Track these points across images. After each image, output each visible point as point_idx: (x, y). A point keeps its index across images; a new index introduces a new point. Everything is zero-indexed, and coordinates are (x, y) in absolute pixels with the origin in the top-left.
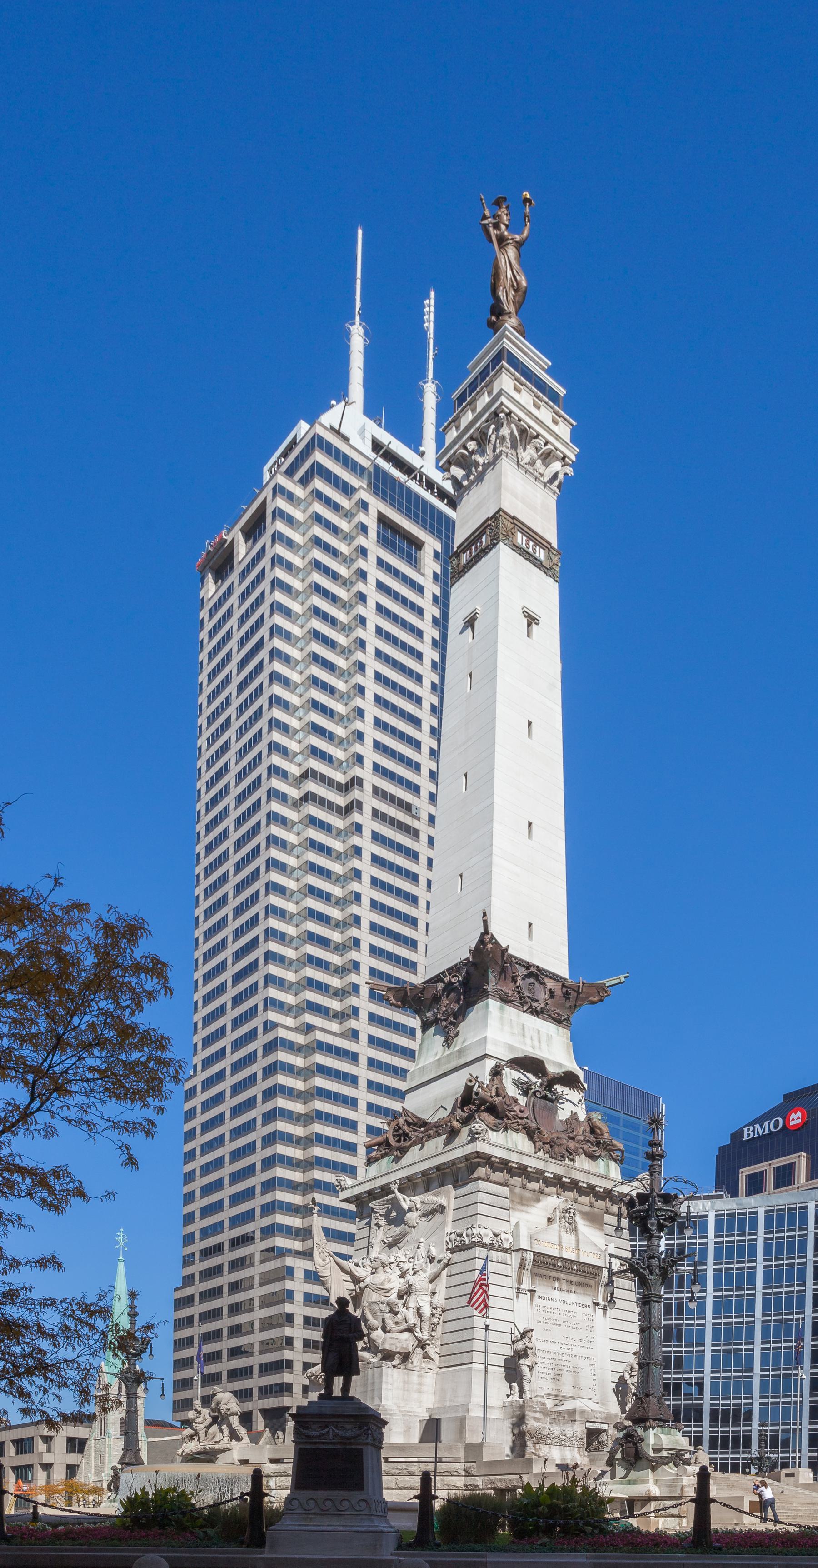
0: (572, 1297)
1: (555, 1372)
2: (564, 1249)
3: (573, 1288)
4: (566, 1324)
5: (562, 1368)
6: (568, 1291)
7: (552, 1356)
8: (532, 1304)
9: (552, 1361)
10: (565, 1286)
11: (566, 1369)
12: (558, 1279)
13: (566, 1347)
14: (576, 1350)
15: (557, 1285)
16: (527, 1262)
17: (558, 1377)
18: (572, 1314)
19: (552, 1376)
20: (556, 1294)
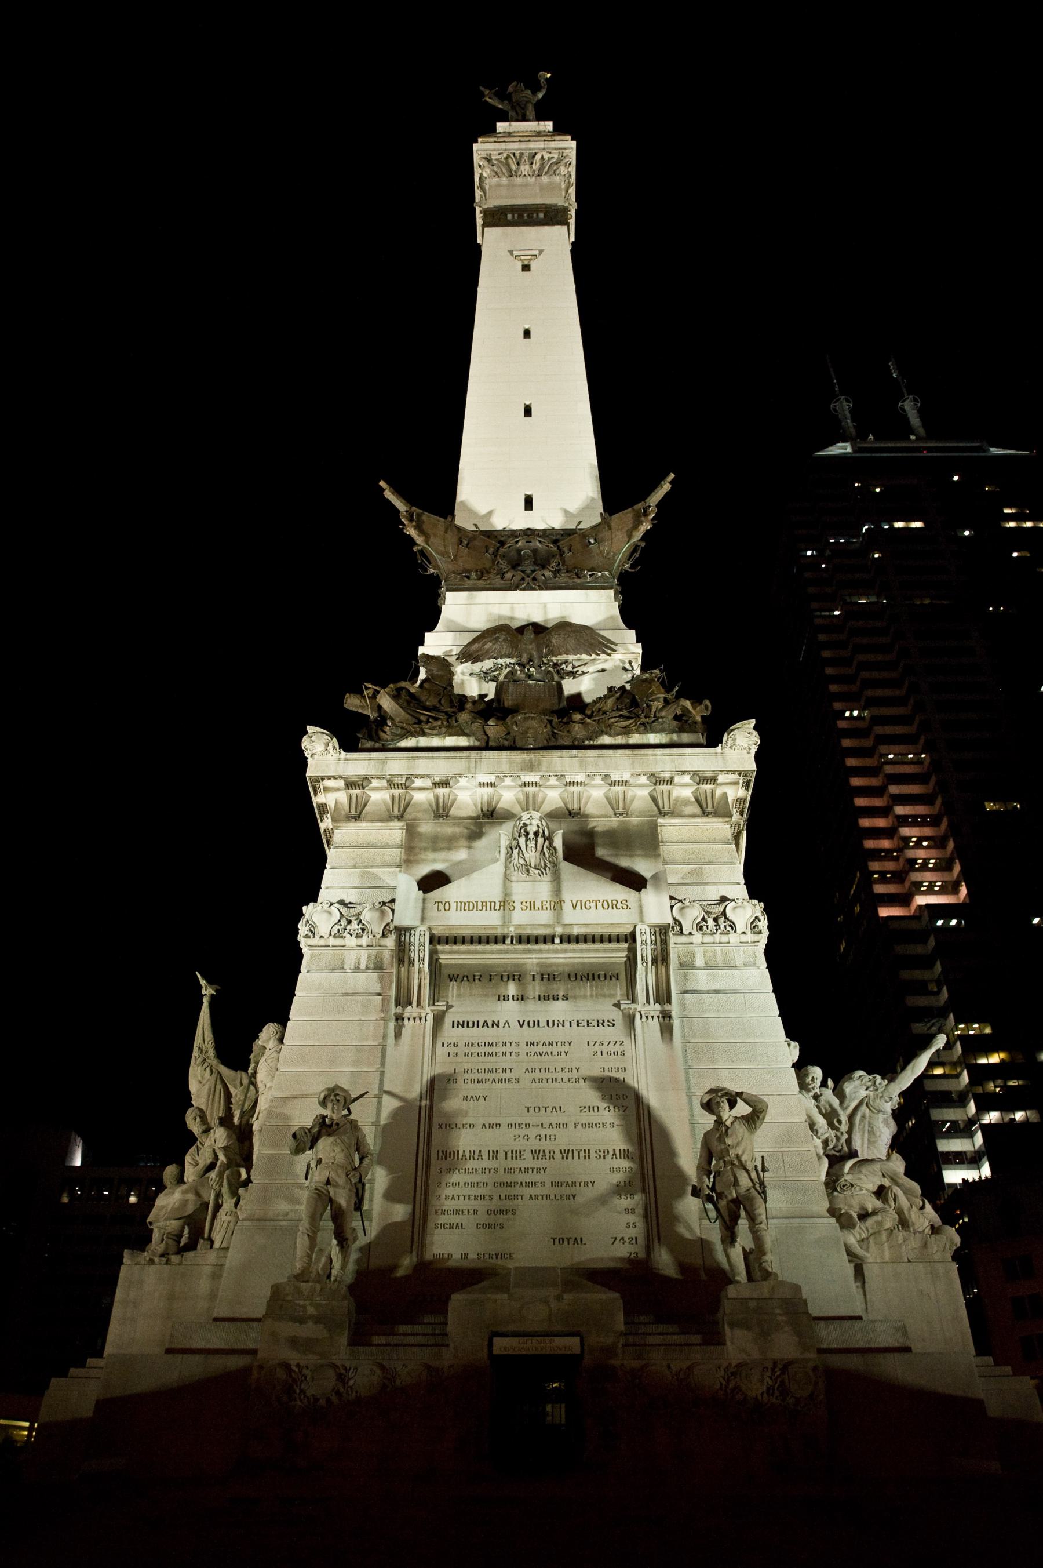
0: (559, 1009)
1: (495, 1205)
4: (537, 1075)
5: (518, 1190)
7: (486, 1163)
8: (434, 1043)
9: (484, 1178)
10: (536, 988)
11: (532, 1191)
13: (533, 1132)
14: (564, 1139)
15: (512, 989)
16: (415, 955)
17: (500, 1219)
18: (554, 1049)
19: (482, 1218)
20: (510, 1011)
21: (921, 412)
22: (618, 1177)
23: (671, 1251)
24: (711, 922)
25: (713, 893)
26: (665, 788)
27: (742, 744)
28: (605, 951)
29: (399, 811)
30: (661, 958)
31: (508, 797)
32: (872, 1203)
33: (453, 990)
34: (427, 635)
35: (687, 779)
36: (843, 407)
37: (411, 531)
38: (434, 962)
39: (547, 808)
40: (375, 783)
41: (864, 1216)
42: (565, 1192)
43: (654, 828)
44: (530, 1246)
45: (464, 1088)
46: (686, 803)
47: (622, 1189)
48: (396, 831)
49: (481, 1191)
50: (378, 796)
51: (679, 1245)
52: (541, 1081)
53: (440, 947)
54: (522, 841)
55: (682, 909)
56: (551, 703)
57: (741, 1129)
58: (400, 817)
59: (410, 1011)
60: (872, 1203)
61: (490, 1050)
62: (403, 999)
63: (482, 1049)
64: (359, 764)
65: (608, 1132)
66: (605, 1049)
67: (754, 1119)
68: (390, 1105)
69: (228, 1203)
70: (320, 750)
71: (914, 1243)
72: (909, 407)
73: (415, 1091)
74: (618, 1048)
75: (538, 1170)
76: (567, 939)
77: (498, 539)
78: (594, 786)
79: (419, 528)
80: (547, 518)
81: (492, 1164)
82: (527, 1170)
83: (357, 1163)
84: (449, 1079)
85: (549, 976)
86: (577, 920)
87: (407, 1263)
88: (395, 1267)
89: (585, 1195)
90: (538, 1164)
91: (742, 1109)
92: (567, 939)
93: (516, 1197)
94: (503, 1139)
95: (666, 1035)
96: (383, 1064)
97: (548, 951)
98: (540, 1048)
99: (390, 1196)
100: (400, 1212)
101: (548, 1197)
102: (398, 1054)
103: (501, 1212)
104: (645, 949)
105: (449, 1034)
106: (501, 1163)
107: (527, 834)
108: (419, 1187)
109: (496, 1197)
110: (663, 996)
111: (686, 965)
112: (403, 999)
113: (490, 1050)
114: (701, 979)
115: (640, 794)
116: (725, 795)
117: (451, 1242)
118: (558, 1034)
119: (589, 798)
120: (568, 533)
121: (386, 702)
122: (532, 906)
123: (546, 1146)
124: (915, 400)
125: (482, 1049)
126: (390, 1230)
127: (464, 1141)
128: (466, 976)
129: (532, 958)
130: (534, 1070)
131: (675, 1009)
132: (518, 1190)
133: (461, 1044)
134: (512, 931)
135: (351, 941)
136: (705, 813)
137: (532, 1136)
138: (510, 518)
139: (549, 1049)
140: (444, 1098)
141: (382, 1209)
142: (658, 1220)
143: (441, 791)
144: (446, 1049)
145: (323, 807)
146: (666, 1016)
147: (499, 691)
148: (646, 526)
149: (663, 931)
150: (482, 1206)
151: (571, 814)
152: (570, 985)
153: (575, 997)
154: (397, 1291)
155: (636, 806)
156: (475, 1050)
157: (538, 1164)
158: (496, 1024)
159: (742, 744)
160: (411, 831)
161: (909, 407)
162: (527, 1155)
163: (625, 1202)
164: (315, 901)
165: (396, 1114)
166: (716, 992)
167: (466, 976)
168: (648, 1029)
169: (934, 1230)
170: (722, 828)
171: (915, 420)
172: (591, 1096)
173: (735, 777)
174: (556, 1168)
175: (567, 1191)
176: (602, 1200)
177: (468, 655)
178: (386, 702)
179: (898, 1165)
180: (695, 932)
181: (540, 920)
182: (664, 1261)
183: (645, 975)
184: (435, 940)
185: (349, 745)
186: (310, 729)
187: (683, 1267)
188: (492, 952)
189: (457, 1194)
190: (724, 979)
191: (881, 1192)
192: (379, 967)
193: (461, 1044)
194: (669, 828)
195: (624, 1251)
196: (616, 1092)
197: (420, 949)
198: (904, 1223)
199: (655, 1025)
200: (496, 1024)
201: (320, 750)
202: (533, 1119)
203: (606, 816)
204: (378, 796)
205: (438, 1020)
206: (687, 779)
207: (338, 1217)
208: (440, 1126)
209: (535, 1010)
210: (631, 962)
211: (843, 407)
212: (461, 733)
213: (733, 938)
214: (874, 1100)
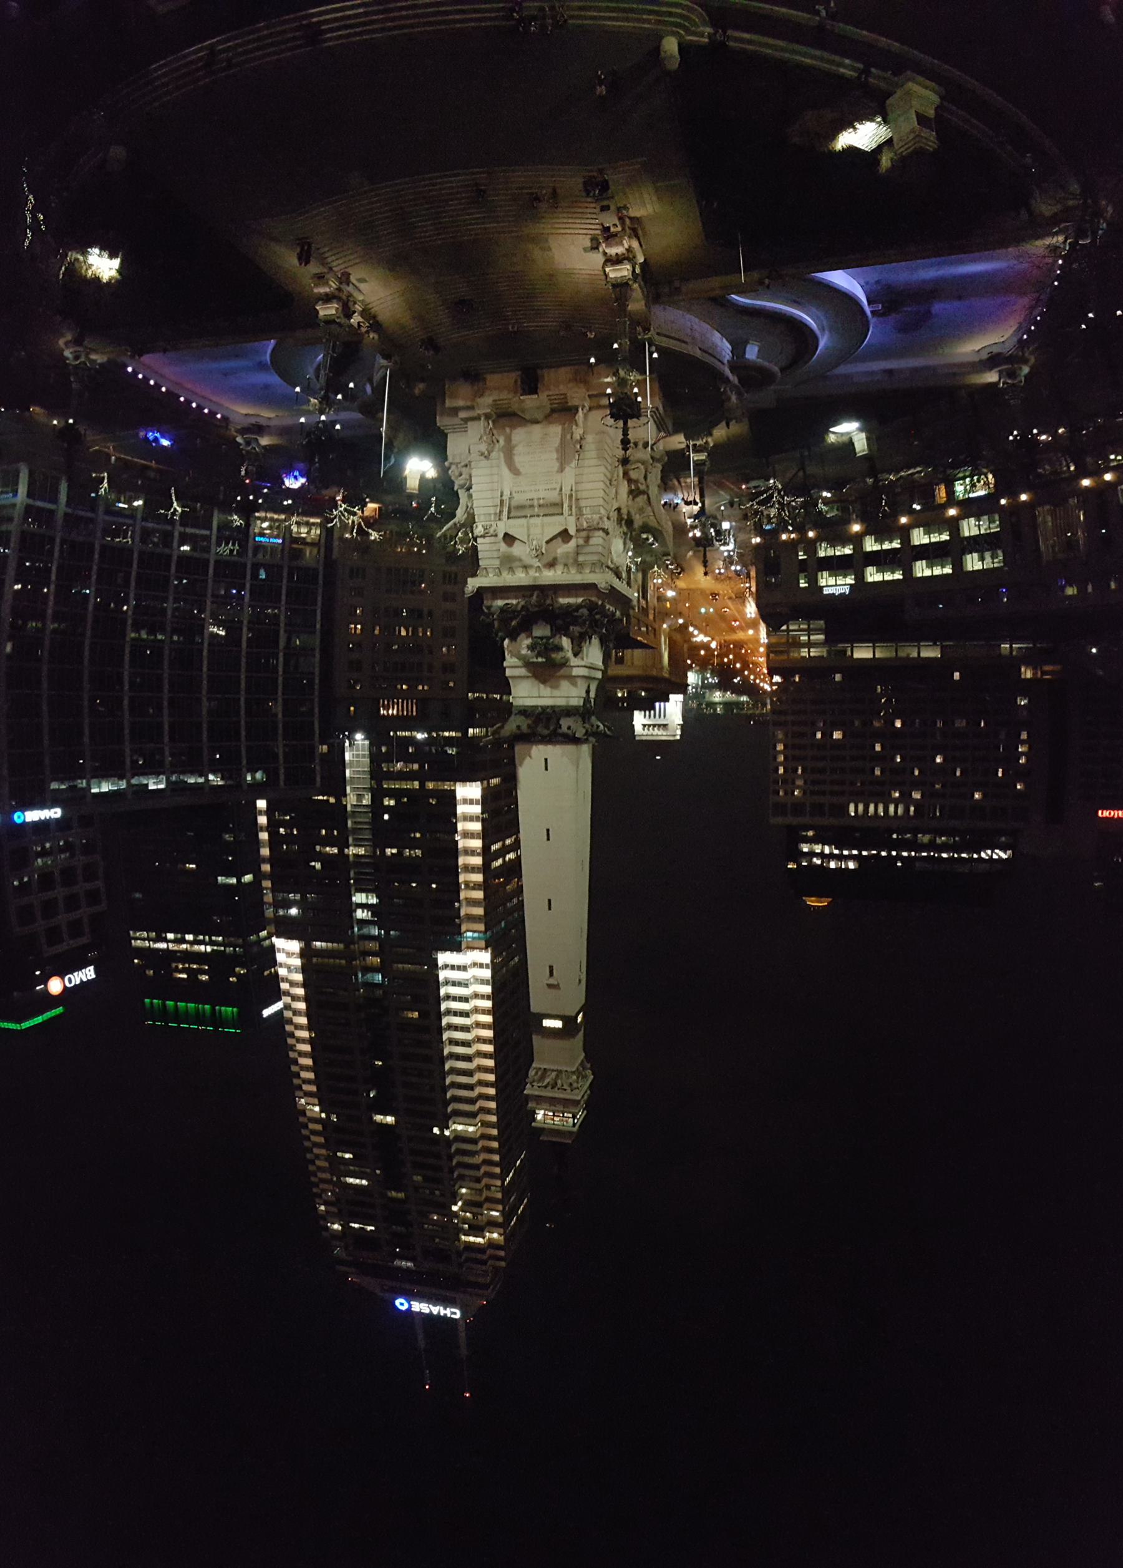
3: (529, 502)
10: (536, 503)
15: (541, 502)
20: (542, 494)
25: (487, 540)
44: (537, 429)
47: (516, 446)
65: (518, 460)
73: (567, 469)
80: (539, 752)
86: (523, 521)
92: (526, 517)
104: (505, 513)
110: (502, 502)
114: (492, 510)
115: (505, 574)
117: (555, 430)
127: (555, 456)
128: (555, 505)
142: (508, 440)
168: (507, 493)
181: (533, 520)
182: (508, 430)
183: (506, 510)
189: (556, 441)
194: (497, 562)
196: (515, 472)
209: (535, 495)
210: (509, 512)
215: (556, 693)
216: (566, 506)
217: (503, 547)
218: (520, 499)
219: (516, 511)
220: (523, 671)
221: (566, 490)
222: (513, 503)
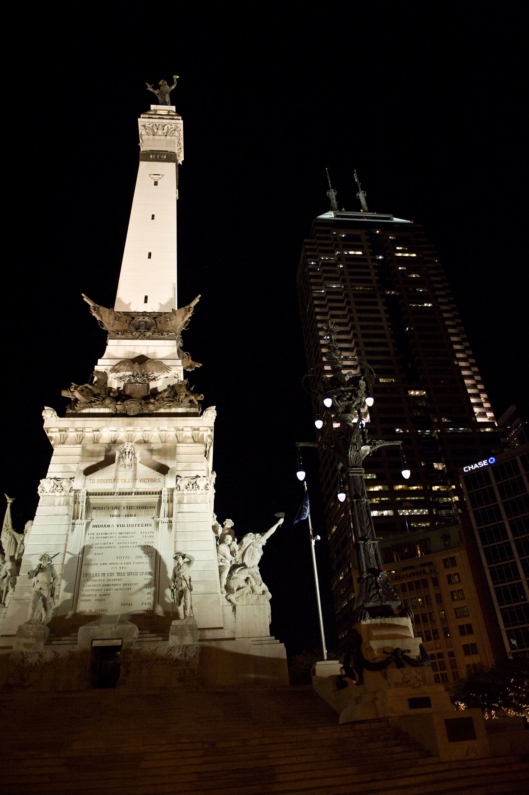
0: (132, 520)
1: (103, 592)
2: (120, 481)
4: (122, 545)
5: (111, 587)
6: (128, 516)
7: (101, 578)
8: (85, 533)
10: (124, 512)
11: (116, 587)
12: (118, 508)
14: (129, 568)
15: (116, 512)
18: (129, 535)
19: (98, 597)
20: (114, 521)
21: (366, 199)
22: (147, 582)
23: (162, 607)
24: (191, 486)
26: (181, 432)
27: (211, 414)
28: (151, 498)
29: (80, 441)
30: (171, 501)
31: (121, 435)
32: (243, 584)
33: (94, 514)
34: (99, 360)
35: (189, 429)
36: (332, 194)
37: (94, 314)
38: (88, 503)
39: (136, 440)
40: (70, 430)
41: (238, 589)
42: (127, 587)
43: (175, 447)
45: (94, 550)
46: (188, 438)
47: (147, 586)
48: (78, 449)
49: (98, 588)
50: (72, 435)
51: (164, 604)
52: (123, 547)
53: (90, 497)
54: (124, 455)
55: (181, 481)
56: (144, 393)
57: (185, 566)
58: (80, 443)
59: (78, 521)
60: (243, 584)
61: (105, 536)
62: (75, 517)
63: (103, 536)
64: (65, 422)
65: (145, 565)
66: (147, 535)
67: (189, 563)
68: (68, 556)
69: (11, 590)
70: (49, 417)
71: (255, 597)
72: (361, 196)
73: (77, 551)
74: (152, 534)
75: (119, 580)
76: (137, 493)
77: (130, 316)
78: (154, 431)
79: (98, 313)
81: (103, 578)
82: (115, 580)
83: (52, 581)
84: (90, 547)
85: (130, 508)
86: (142, 487)
87: (70, 613)
88: (66, 615)
89: (134, 588)
90: (119, 577)
91: (186, 560)
92: (137, 493)
93: (110, 590)
94: (107, 569)
95: (170, 529)
96: (67, 541)
97: (130, 498)
98: (124, 535)
99: (66, 590)
100: (69, 596)
101: (121, 589)
102: (72, 537)
103: (104, 595)
104: (165, 497)
105: (91, 530)
106: (106, 577)
107: (126, 452)
108: (76, 588)
109: (103, 590)
111: (180, 502)
112: (75, 517)
113: (105, 536)
114: (185, 507)
115: (172, 434)
116: (203, 435)
117: (86, 606)
118: (131, 529)
119: (152, 436)
120: (160, 314)
121: (77, 395)
122: (125, 481)
123: (123, 571)
124: (364, 193)
125: (103, 536)
126: (66, 602)
127: (93, 570)
128: (100, 508)
129: (124, 501)
130: (121, 543)
131: (173, 519)
132: (111, 587)
133: (95, 534)
134: (117, 491)
135: (58, 494)
136: (195, 442)
137: (118, 568)
138: (137, 306)
139: (127, 535)
140: (88, 554)
141: (63, 595)
142: (158, 597)
143: (96, 433)
144: (90, 536)
145: (51, 437)
146: (170, 522)
147: (124, 387)
148: (189, 315)
149: (172, 490)
150: (98, 593)
151: (145, 442)
152: (137, 510)
153: (138, 515)
154: (64, 624)
155: (170, 439)
156: (101, 536)
157: (119, 577)
158: (109, 526)
159: (211, 414)
160: (83, 448)
161: (361, 196)
162: (116, 574)
163: (148, 590)
164: (45, 478)
165: (70, 560)
166: (190, 512)
167: (100, 508)
168: (164, 527)
169: (264, 592)
170: (201, 448)
171: (363, 202)
172: (141, 553)
173: (206, 428)
174: (125, 579)
175: (128, 587)
176: (141, 590)
177: (114, 370)
178: (77, 395)
179: (257, 569)
180: (184, 489)
181: (126, 487)
182: (159, 610)
183: (164, 506)
184: (88, 494)
185: (62, 414)
186: (46, 408)
187: (165, 613)
188: (109, 498)
189: (89, 589)
190: (193, 507)
191: (247, 580)
192: (68, 504)
193: (95, 534)
194: (181, 448)
195: (146, 607)
197: (82, 497)
198: (253, 591)
199: (166, 525)
200: (109, 526)
201: (49, 417)
202: (119, 561)
203: (158, 443)
204: (72, 435)
205: (88, 525)
206: (189, 429)
207: (44, 600)
208: (85, 565)
210: (160, 502)
211: (332, 194)
212: (107, 407)
213: (198, 492)
214: (255, 544)
215: (131, 349)
216: (82, 506)
217: (169, 464)
218: (145, 518)
219: (154, 506)
220: (167, 363)
221: (81, 523)
222: (154, 512)
